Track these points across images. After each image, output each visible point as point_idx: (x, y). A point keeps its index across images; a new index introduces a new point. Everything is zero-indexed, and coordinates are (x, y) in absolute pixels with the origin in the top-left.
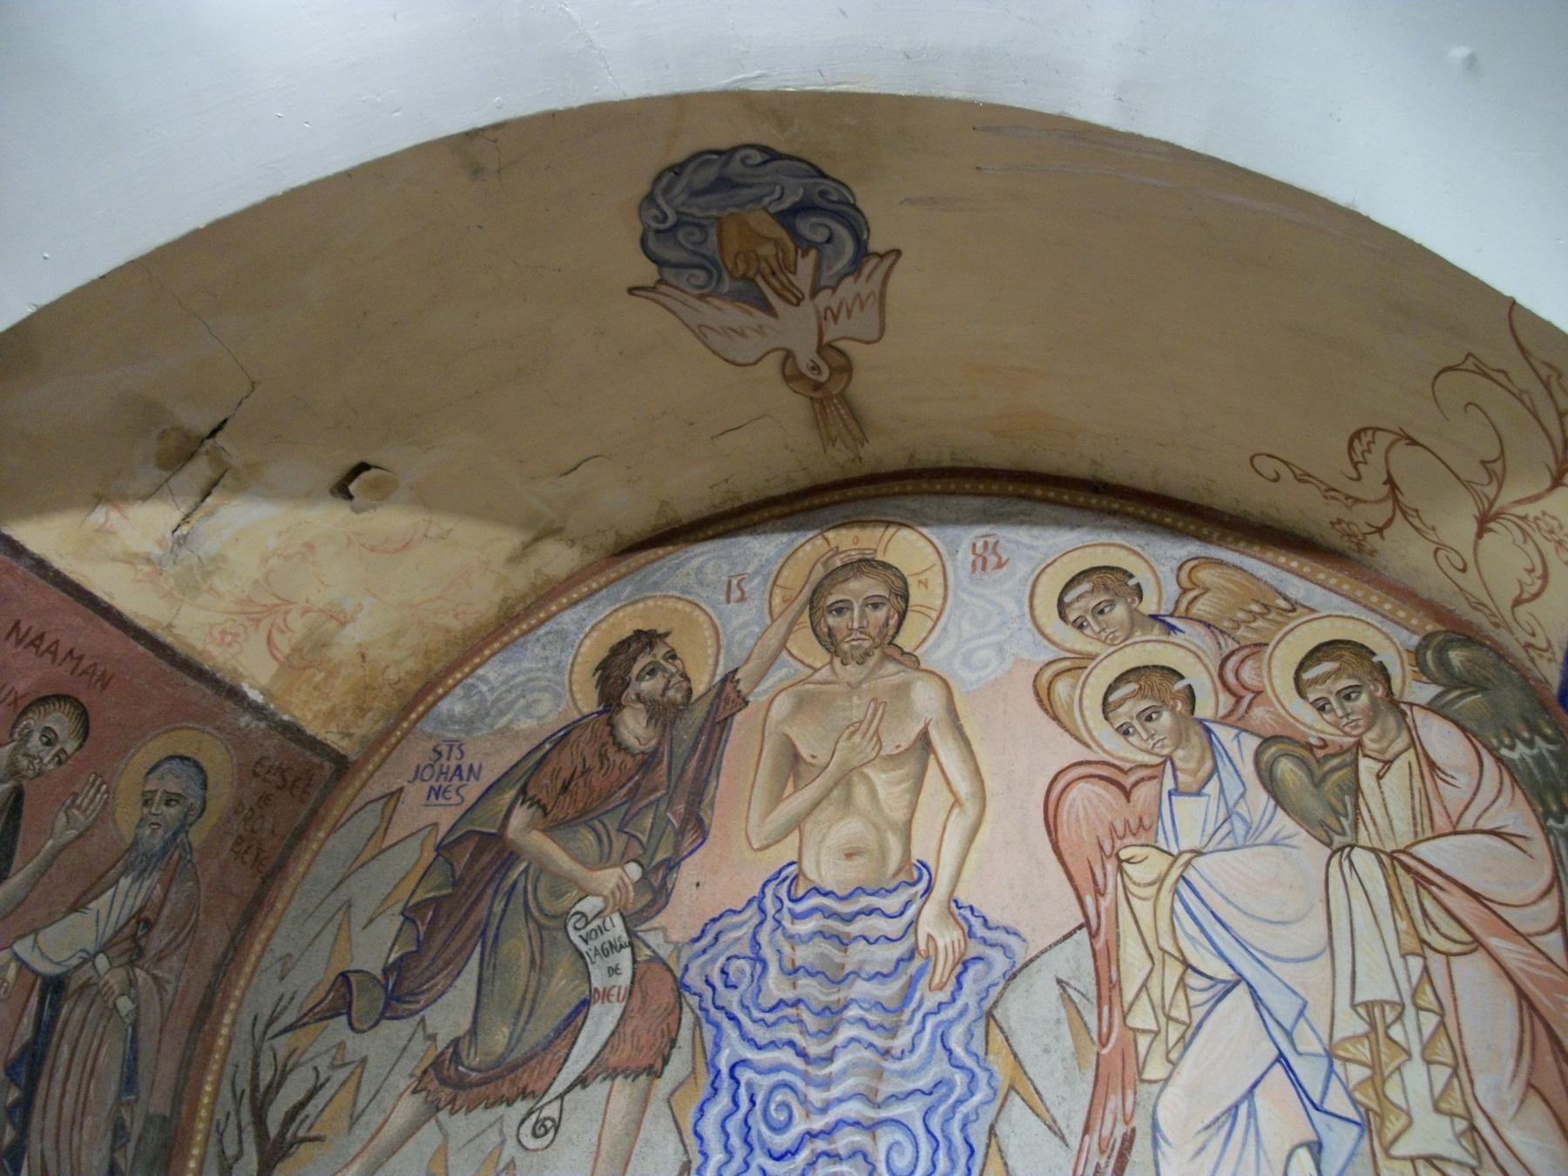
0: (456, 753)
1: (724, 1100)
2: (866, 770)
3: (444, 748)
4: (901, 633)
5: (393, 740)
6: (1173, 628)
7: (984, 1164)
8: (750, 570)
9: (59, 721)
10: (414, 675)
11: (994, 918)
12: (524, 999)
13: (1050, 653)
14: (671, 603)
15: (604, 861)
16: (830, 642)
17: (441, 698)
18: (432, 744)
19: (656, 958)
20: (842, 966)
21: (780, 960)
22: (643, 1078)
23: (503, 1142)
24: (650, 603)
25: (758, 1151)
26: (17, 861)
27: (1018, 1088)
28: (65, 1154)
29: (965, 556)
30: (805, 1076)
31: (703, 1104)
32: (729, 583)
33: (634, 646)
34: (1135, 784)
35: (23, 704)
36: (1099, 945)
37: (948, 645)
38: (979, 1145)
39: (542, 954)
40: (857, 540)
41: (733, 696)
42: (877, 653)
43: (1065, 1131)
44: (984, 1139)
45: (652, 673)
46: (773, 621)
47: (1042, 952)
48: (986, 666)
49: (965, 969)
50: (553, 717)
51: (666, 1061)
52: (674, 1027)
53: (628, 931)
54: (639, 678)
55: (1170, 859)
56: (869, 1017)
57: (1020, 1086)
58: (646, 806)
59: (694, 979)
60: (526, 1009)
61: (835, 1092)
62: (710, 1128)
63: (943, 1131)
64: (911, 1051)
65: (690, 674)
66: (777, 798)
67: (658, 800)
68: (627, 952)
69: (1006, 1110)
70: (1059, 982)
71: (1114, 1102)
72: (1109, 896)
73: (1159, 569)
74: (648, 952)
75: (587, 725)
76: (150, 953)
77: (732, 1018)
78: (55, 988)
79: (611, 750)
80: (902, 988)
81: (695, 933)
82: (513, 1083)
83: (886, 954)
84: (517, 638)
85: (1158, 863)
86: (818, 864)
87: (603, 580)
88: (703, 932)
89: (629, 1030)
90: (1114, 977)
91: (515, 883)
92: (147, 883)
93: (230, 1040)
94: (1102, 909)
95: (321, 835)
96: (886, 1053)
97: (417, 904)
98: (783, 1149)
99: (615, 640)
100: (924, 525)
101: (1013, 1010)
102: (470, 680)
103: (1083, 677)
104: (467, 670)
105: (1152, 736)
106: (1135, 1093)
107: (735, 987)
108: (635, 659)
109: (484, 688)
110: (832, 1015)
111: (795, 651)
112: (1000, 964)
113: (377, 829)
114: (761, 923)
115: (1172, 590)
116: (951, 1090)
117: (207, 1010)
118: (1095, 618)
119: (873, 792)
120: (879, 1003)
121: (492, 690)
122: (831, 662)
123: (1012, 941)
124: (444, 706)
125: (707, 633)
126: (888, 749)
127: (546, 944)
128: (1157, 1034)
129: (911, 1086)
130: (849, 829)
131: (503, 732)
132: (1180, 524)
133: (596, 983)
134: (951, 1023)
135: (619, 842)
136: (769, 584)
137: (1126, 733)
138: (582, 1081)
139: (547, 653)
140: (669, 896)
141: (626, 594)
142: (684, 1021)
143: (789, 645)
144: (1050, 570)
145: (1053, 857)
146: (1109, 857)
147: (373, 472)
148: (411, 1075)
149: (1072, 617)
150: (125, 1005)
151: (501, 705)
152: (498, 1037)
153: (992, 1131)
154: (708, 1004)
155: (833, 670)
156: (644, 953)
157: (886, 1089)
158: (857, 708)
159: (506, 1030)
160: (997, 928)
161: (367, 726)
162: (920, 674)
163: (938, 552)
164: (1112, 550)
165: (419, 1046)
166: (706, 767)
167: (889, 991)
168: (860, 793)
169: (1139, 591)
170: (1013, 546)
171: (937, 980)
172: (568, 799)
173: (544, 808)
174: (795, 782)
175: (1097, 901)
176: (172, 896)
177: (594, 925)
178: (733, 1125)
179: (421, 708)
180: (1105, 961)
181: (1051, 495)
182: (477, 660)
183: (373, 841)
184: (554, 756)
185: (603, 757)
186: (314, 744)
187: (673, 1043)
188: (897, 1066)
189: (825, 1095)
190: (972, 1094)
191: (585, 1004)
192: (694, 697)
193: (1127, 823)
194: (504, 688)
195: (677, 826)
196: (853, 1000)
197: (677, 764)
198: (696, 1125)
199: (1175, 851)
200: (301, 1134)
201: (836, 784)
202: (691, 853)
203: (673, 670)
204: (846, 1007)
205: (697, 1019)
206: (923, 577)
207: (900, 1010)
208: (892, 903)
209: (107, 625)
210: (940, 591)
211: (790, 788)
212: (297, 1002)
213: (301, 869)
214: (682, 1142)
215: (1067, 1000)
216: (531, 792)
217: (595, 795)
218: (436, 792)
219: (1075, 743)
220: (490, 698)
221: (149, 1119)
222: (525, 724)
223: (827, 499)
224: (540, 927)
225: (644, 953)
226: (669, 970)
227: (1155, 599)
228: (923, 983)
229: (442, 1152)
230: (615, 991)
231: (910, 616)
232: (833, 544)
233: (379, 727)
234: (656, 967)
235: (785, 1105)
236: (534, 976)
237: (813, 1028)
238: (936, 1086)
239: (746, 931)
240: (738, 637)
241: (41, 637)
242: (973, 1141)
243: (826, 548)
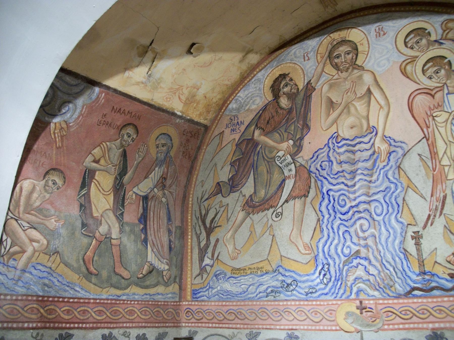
0: (236, 118)
1: (326, 201)
2: (353, 102)
3: (233, 118)
4: (357, 60)
5: (218, 118)
6: (442, 43)
7: (403, 209)
8: (309, 50)
9: (130, 130)
10: (220, 99)
11: (397, 139)
12: (267, 182)
13: (404, 58)
14: (288, 65)
15: (282, 141)
16: (336, 67)
17: (229, 104)
18: (229, 117)
19: (301, 165)
20: (354, 159)
21: (336, 160)
22: (303, 198)
23: (268, 220)
24: (282, 66)
25: (338, 213)
26: (129, 169)
27: (410, 186)
28: (157, 239)
29: (373, 33)
30: (348, 191)
31: (321, 202)
32: (304, 55)
33: (280, 79)
34: (435, 93)
35: (120, 128)
36: (430, 142)
37: (372, 61)
38: (401, 203)
39: (270, 169)
40: (339, 35)
42: (351, 68)
43: (426, 197)
44: (402, 202)
45: (286, 86)
46: (319, 64)
47: (413, 147)
48: (384, 66)
49: (390, 155)
50: (261, 103)
51: (309, 192)
52: (309, 183)
53: (292, 159)
54: (283, 88)
55: (449, 114)
56: (364, 172)
57: (411, 186)
58: (291, 124)
59: (313, 169)
60: (268, 184)
61: (357, 194)
62: (323, 209)
63: (389, 201)
64: (378, 180)
65: (297, 84)
66: (328, 115)
67: (294, 121)
68: (293, 164)
69: (407, 193)
70: (419, 155)
71: (439, 187)
72: (431, 128)
73: (435, 26)
74: (299, 164)
75: (271, 104)
76: (167, 186)
77: (325, 178)
78: (145, 198)
80: (373, 163)
81: (311, 156)
82: (268, 204)
83: (366, 154)
84: (246, 83)
85: (445, 116)
86: (343, 131)
87: (267, 62)
88: (313, 156)
89: (297, 186)
90: (435, 151)
91: (259, 151)
92: (162, 168)
93: (192, 204)
94: (429, 132)
95: (205, 147)
96: (370, 182)
97: (234, 161)
98: (345, 212)
99: (274, 78)
100: (359, 26)
101: (406, 165)
102: (236, 98)
103: (415, 64)
104: (235, 95)
105: (439, 78)
106: (445, 184)
107: (325, 170)
108: (281, 83)
109: (240, 99)
110: (353, 173)
111: (326, 72)
112: (400, 152)
114: (329, 151)
115: (440, 31)
116: (391, 189)
117: (185, 198)
118: (416, 45)
119: (356, 109)
120: (366, 168)
121: (243, 99)
122: (338, 73)
123: (403, 145)
124: (230, 106)
125: (300, 71)
126: (359, 95)
127: (271, 166)
128: (450, 166)
129: (379, 190)
130: (351, 120)
131: (248, 110)
132: (440, 10)
133: (286, 175)
134: (388, 171)
136: (316, 54)
137: (431, 78)
138: (287, 201)
139: (256, 86)
140: (302, 147)
141: (275, 64)
142: (312, 181)
143: (324, 70)
144: (400, 32)
145: (412, 119)
146: (430, 116)
147: (197, 45)
148: (241, 206)
149: (409, 46)
150: (164, 200)
151: (246, 103)
152: (262, 193)
153: (404, 200)
154: (318, 175)
155: (339, 75)
156: (298, 164)
157: (372, 192)
158: (348, 85)
159: (264, 191)
160: (398, 142)
161: (211, 116)
162: (365, 72)
163: (365, 34)
164: (419, 22)
165: (241, 198)
166: (307, 110)
167: (369, 164)
168: (352, 109)
169: (429, 34)
170: (388, 28)
171: (382, 159)
173: (263, 129)
174: (333, 109)
175: (427, 130)
176: (169, 170)
177: (282, 159)
178: (330, 207)
179: (224, 108)
180: (432, 148)
181: (397, 9)
182: (237, 92)
183: (218, 147)
184: (263, 115)
186: (197, 123)
187: (310, 187)
188: (374, 185)
189: (355, 196)
190: (397, 190)
191: (284, 180)
192: (300, 90)
193: (434, 105)
194: (246, 98)
195: (301, 127)
196: (359, 168)
197: (298, 110)
198: (319, 208)
199: (450, 111)
200: (215, 225)
201: (345, 108)
202: (306, 135)
203: (292, 84)
204: (357, 170)
205: (315, 180)
206: (361, 43)
207: (373, 169)
208: (366, 139)
209: (136, 103)
210: (367, 45)
211: (331, 111)
212: (207, 192)
213: (201, 157)
214: (316, 213)
215: (422, 159)
216: (259, 125)
217: (277, 123)
218: (233, 130)
219: (415, 84)
220: (242, 102)
221: (176, 227)
222: (254, 107)
223: (328, 25)
224: (268, 162)
225: (298, 164)
226: (306, 168)
227: (435, 35)
228: (378, 160)
229: (252, 225)
230: (291, 176)
231: (359, 55)
232: (333, 38)
233: (214, 116)
234: (302, 168)
235: (344, 200)
236: (269, 175)
237: (348, 177)
238: (386, 189)
239: (325, 154)
240: (309, 71)
241: (120, 109)
242: (398, 203)
243: (331, 39)
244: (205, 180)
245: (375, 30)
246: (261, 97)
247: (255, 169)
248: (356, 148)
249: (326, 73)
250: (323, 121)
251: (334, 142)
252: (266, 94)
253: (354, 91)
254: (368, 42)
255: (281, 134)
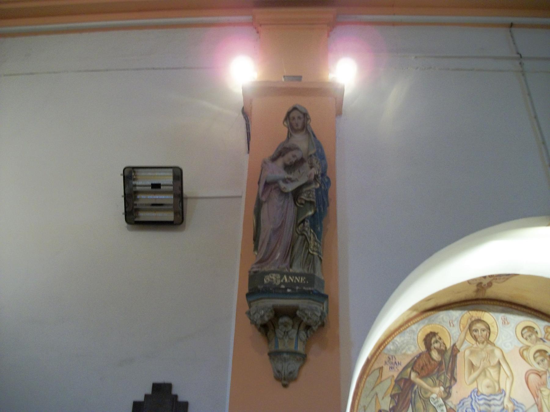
0: (394, 358)
6: (544, 341)
8: (454, 319)
13: (521, 345)
15: (435, 385)
16: (475, 338)
19: (451, 408)
33: (431, 336)
41: (456, 349)
45: (436, 342)
53: (443, 401)
54: (434, 343)
66: (470, 374)
67: (444, 373)
79: (431, 360)
86: (482, 388)
88: (460, 403)
91: (415, 391)
102: (393, 341)
108: (431, 338)
109: (397, 343)
111: (468, 340)
113: (379, 376)
115: (543, 333)
119: (490, 374)
121: (399, 343)
126: (492, 364)
127: (426, 405)
130: (486, 381)
135: (437, 382)
136: (459, 323)
140: (451, 394)
143: (466, 338)
149: (525, 336)
155: (477, 345)
156: (448, 407)
158: (484, 354)
168: (488, 374)
172: (423, 371)
174: (473, 370)
185: (430, 362)
208: (498, 398)
210: (496, 328)
216: (414, 369)
218: (391, 368)
222: (409, 353)
224: (424, 401)
225: (448, 407)
239: (469, 403)
244: (367, 405)
245: (502, 319)
246: (415, 347)
247: (413, 404)
248: (492, 402)
249: (467, 340)
250: (466, 377)
251: (475, 394)
252: (419, 345)
253: (489, 360)
254: (497, 325)
255: (434, 381)
